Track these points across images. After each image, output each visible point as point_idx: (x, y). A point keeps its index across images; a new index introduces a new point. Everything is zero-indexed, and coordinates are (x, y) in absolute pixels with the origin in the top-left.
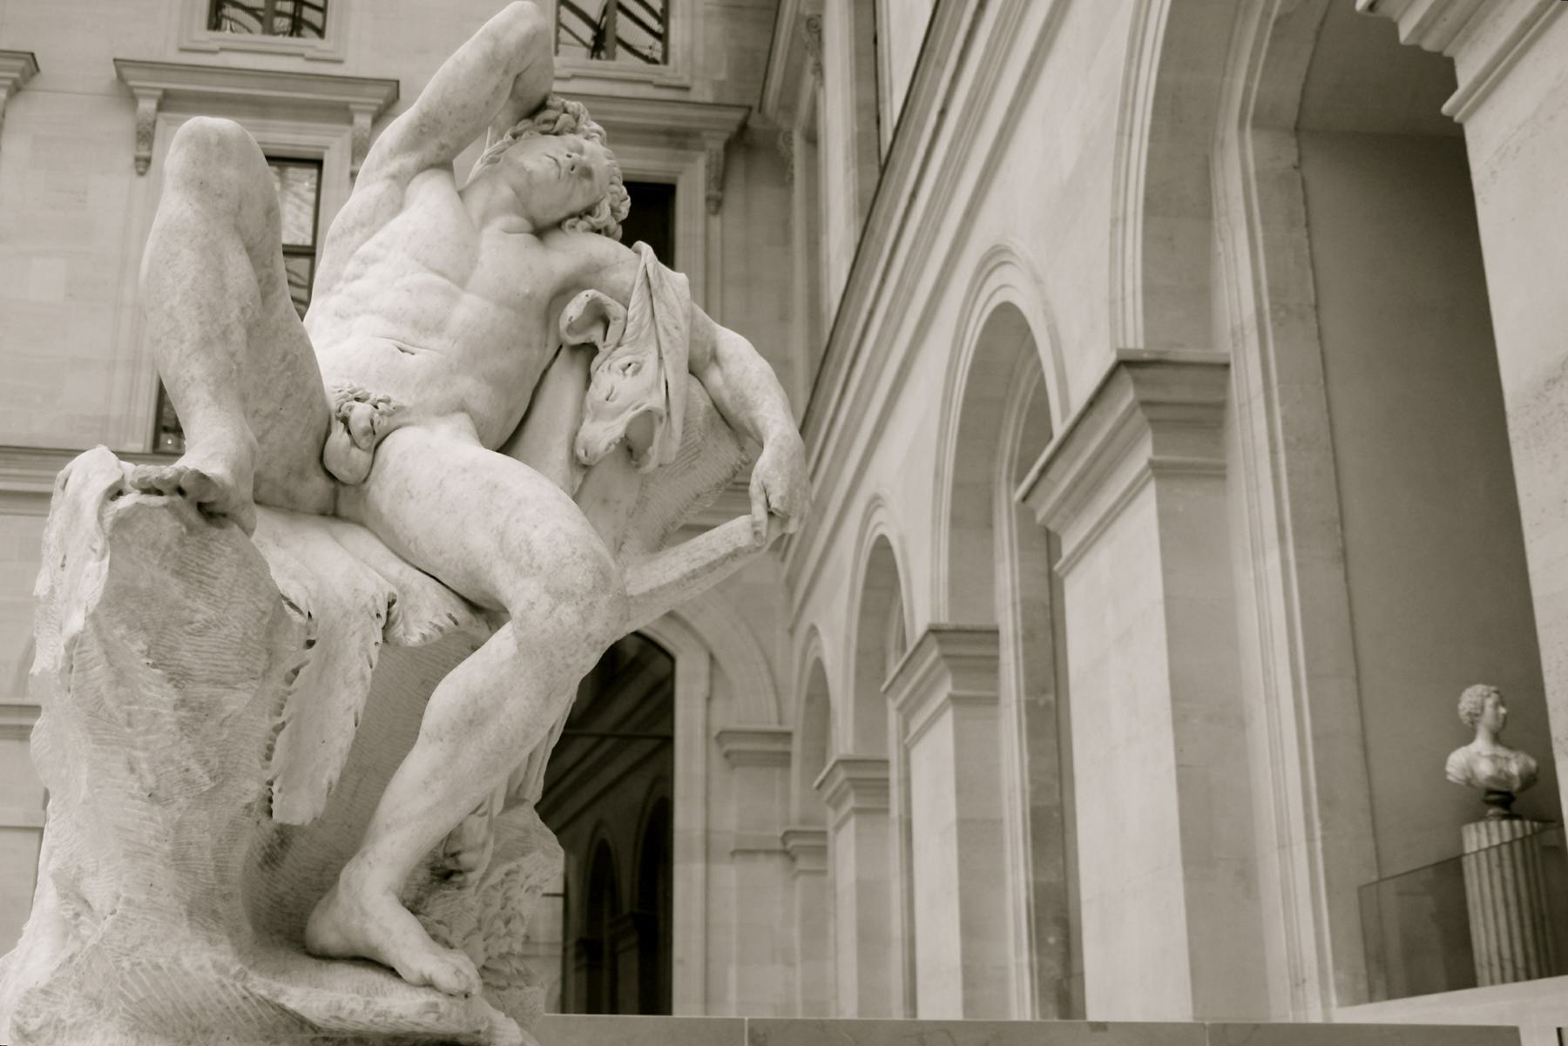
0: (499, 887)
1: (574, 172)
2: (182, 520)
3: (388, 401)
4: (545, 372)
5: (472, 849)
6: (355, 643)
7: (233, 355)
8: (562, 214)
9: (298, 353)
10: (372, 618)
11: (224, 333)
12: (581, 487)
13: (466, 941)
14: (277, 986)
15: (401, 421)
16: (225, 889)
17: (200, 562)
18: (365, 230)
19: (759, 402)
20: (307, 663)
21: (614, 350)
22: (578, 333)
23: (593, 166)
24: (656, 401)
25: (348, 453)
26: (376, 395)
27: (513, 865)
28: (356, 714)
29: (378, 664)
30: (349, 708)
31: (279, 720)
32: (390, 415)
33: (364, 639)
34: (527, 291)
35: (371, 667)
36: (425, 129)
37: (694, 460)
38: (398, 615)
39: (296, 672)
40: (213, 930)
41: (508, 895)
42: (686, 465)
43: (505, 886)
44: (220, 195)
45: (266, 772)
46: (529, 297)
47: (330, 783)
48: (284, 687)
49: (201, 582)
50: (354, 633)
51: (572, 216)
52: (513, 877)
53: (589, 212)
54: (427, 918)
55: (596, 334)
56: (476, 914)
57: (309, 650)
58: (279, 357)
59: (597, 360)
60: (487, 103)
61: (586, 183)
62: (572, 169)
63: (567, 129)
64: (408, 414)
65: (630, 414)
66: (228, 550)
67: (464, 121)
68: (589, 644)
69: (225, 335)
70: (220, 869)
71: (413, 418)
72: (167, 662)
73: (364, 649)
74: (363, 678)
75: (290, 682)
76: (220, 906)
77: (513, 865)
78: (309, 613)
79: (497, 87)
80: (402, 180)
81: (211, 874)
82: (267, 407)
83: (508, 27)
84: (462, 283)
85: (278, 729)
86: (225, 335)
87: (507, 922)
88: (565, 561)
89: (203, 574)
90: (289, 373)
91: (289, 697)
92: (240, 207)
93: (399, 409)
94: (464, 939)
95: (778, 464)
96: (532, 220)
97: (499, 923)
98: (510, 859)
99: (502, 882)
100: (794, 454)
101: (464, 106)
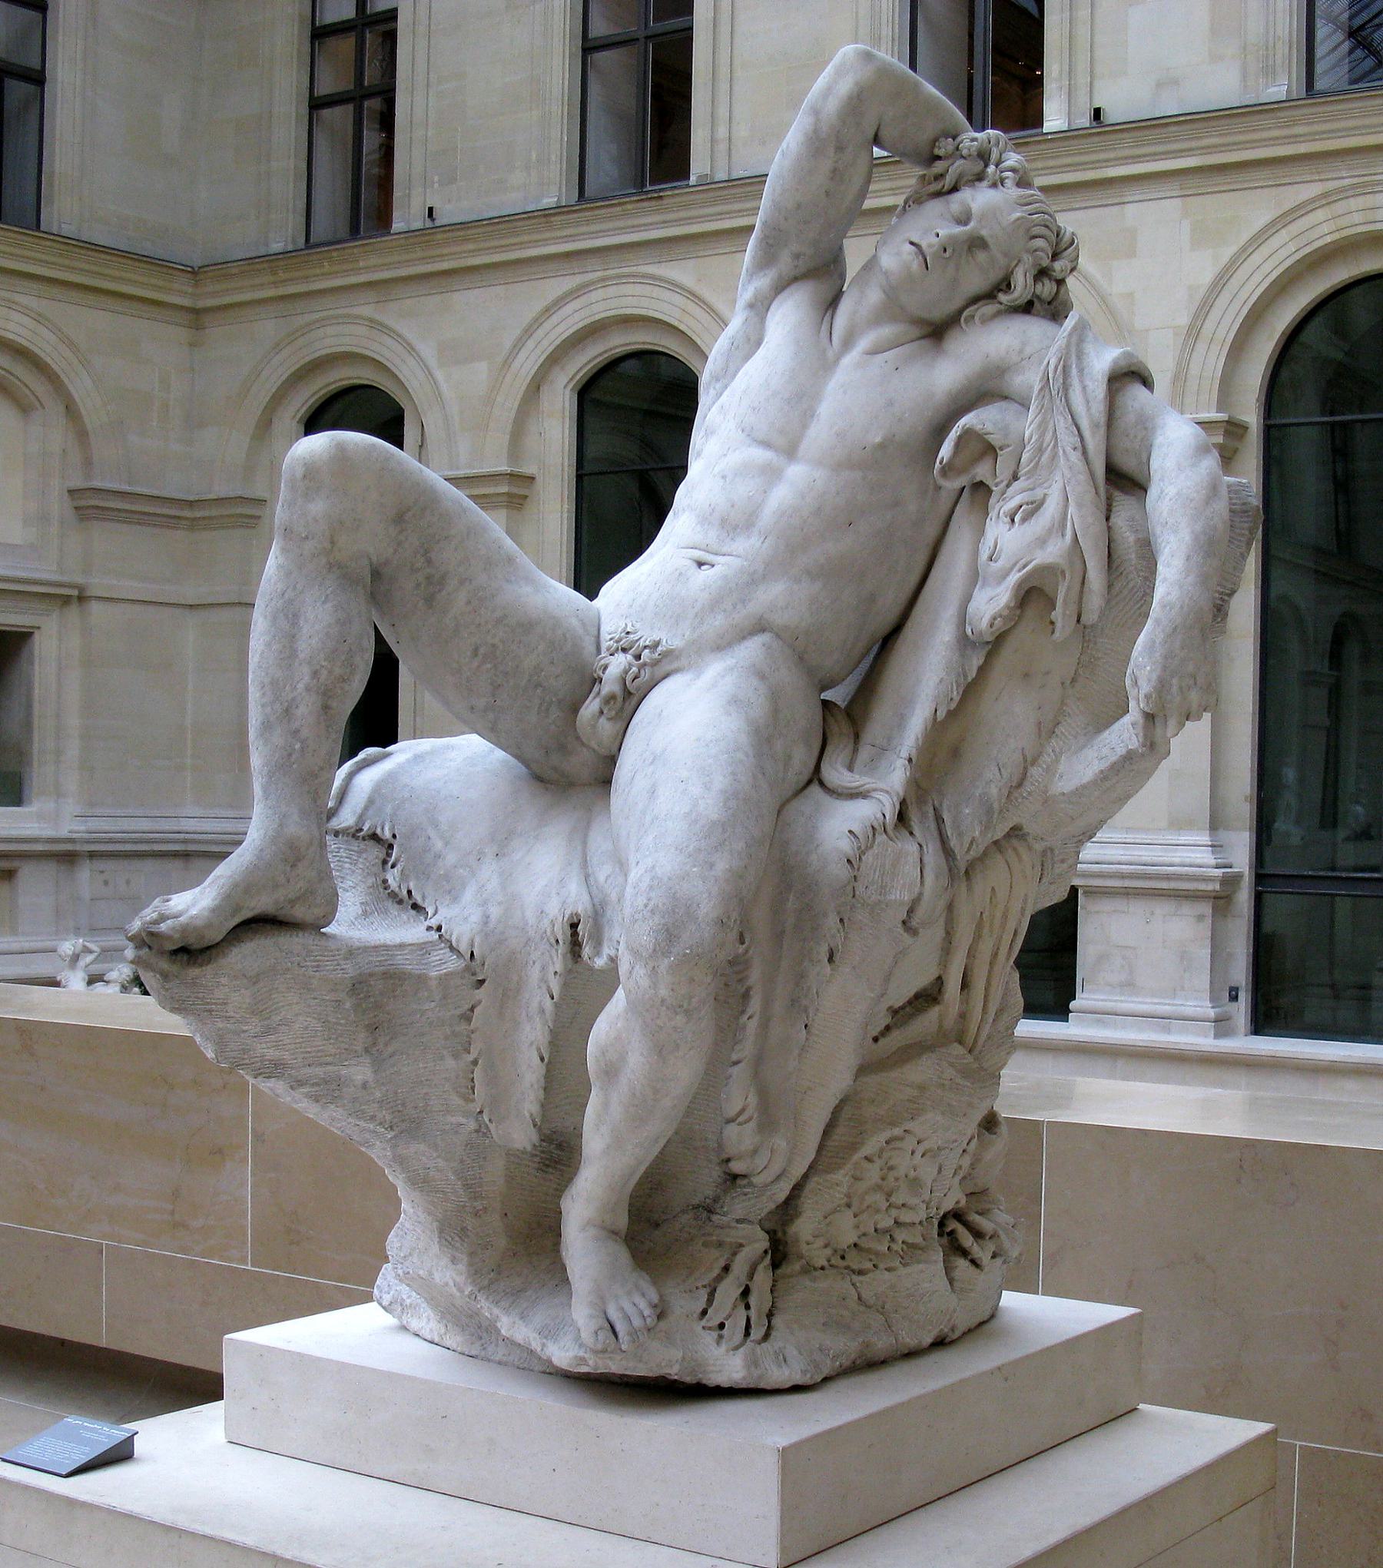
0: (876, 1158)
1: (947, 254)
2: (153, 970)
3: (657, 644)
4: (952, 512)
5: (740, 1157)
6: (535, 973)
7: (297, 731)
8: (957, 303)
9: (496, 641)
10: (551, 945)
11: (287, 711)
12: (982, 670)
13: (828, 1220)
14: (496, 1311)
15: (675, 665)
16: (478, 1205)
17: (201, 995)
18: (718, 386)
19: (1163, 545)
20: (480, 1002)
21: (1008, 486)
22: (961, 472)
23: (984, 233)
24: (1053, 552)
25: (594, 727)
26: (647, 637)
27: (897, 1131)
28: (539, 1049)
29: (561, 998)
30: (532, 1044)
31: (471, 1057)
32: (656, 663)
33: (543, 968)
34: (878, 440)
35: (553, 998)
36: (771, 242)
37: (1142, 606)
38: (584, 935)
39: (472, 1009)
40: (457, 1249)
41: (891, 1163)
42: (1135, 612)
43: (886, 1155)
44: (307, 538)
45: (471, 1105)
46: (882, 446)
47: (532, 1115)
48: (463, 1027)
49: (210, 1011)
50: (534, 963)
51: (976, 300)
52: (898, 1144)
53: (1005, 284)
54: (724, 1218)
55: (982, 472)
56: (845, 1189)
57: (477, 991)
58: (469, 653)
59: (992, 501)
60: (827, 194)
61: (981, 256)
62: (945, 250)
63: (965, 179)
64: (678, 658)
65: (1014, 577)
66: (224, 980)
67: (805, 223)
68: (668, 1008)
69: (288, 712)
70: (473, 1188)
71: (684, 662)
72: (247, 1061)
73: (543, 980)
74: (542, 1011)
75: (469, 1020)
76: (470, 1222)
77: (897, 1131)
78: (472, 953)
79: (835, 171)
80: (760, 307)
81: (461, 1192)
82: (481, 703)
83: (828, 91)
84: (790, 452)
85: (475, 1063)
86: (288, 712)
87: (889, 1195)
88: (636, 917)
89: (208, 1003)
90: (489, 666)
91: (473, 1036)
92: (333, 542)
93: (668, 654)
94: (826, 1218)
95: (1151, 647)
96: (918, 322)
97: (879, 1199)
98: (893, 1124)
99: (882, 1150)
100: (1175, 629)
101: (799, 206)
